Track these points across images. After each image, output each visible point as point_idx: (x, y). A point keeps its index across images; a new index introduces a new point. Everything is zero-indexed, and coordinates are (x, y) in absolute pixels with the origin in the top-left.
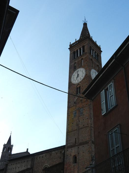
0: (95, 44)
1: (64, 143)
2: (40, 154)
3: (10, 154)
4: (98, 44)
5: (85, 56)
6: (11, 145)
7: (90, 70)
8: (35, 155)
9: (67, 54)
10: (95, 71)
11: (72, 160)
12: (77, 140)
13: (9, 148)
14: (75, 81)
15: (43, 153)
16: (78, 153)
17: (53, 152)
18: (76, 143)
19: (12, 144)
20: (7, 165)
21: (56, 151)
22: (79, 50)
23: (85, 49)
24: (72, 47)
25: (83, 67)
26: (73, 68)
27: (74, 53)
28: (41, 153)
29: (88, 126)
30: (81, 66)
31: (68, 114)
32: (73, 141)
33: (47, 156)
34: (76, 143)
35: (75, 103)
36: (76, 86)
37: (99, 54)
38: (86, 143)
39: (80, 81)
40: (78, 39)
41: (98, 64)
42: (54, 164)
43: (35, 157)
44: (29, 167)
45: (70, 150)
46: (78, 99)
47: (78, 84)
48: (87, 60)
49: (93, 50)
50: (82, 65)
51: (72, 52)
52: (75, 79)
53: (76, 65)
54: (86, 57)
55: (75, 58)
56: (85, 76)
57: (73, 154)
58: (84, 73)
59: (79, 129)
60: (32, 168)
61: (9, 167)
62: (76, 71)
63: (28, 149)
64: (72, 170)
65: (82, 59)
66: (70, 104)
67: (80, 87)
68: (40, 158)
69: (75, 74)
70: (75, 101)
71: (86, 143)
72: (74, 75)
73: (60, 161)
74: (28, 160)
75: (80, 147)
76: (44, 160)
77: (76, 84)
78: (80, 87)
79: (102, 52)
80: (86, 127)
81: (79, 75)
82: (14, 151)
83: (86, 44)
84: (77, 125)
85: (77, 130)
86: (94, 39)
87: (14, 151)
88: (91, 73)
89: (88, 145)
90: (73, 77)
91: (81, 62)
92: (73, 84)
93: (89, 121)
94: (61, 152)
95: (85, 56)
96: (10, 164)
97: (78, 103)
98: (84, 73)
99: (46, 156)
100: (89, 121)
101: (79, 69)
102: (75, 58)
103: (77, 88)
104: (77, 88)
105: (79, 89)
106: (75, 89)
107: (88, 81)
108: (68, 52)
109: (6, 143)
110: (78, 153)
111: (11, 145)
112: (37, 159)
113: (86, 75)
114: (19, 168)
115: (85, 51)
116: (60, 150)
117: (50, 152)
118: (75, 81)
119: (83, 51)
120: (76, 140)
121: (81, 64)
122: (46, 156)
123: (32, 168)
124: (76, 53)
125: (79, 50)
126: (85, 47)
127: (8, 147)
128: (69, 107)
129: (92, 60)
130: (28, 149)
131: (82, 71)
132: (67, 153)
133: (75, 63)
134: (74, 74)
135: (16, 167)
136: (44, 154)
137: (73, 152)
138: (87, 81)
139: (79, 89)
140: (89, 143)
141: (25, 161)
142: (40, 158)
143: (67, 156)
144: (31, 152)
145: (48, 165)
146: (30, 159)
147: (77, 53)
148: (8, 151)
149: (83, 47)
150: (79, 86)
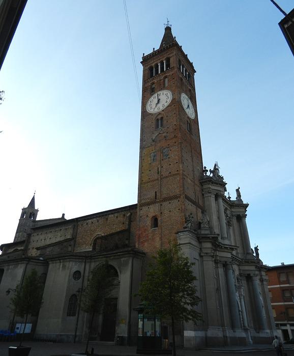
1: (134, 201)
2: (88, 219)
3: (35, 221)
5: (171, 73)
6: (36, 209)
7: (180, 94)
8: (80, 221)
9: (139, 70)
10: (186, 97)
11: (149, 222)
12: (157, 194)
13: (31, 213)
14: (154, 107)
15: (94, 218)
16: (161, 213)
17: (110, 216)
18: (156, 198)
19: (36, 208)
20: (29, 235)
21: (116, 215)
22: (159, 64)
24: (146, 60)
25: (167, 89)
26: (149, 90)
27: (151, 69)
28: (89, 218)
29: (178, 174)
30: (163, 87)
31: (141, 157)
32: (151, 195)
33: (100, 221)
34: (156, 198)
35: (153, 141)
36: (155, 116)
38: (176, 197)
39: (161, 108)
40: (157, 48)
42: (113, 231)
43: (79, 223)
44: (69, 237)
45: (145, 209)
46: (160, 135)
47: (160, 114)
48: (175, 79)
49: (183, 67)
50: (166, 85)
52: (154, 106)
53: (154, 86)
54: (173, 74)
55: (152, 76)
57: (151, 215)
58: (170, 97)
59: (161, 179)
60: (74, 238)
61: (32, 238)
62: (156, 95)
63: (63, 215)
64: (150, 237)
65: (166, 77)
66: (144, 143)
67: (162, 118)
68: (87, 224)
69: (153, 100)
70: (154, 138)
71: (176, 197)
73: (123, 228)
74: (67, 227)
75: (164, 204)
76: (95, 227)
77: (155, 114)
78: (162, 118)
80: (176, 174)
81: (161, 101)
82: (39, 218)
84: (158, 173)
85: (158, 179)
87: (39, 218)
88: (182, 98)
89: (179, 201)
90: (149, 103)
91: (164, 81)
92: (150, 114)
93: (181, 167)
94: (124, 215)
95: (171, 73)
96: (35, 234)
97: (160, 141)
98: (170, 97)
99: (98, 221)
100: (181, 167)
101: (161, 92)
102: (152, 76)
103: (158, 119)
106: (154, 121)
107: (177, 109)
108: (141, 68)
109: (26, 206)
110: (161, 213)
111: (36, 209)
112: (82, 225)
113: (173, 100)
114: (50, 239)
115: (171, 64)
116: (123, 213)
117: (106, 215)
119: (168, 66)
120: (156, 195)
121: (164, 84)
122: (98, 221)
123: (74, 238)
125: (159, 64)
126: (171, 60)
127: (30, 212)
128: (142, 148)
129: (182, 80)
130: (63, 215)
131: (167, 95)
132: (140, 214)
133: (153, 83)
134: (152, 98)
135: (46, 238)
136: (95, 219)
137: (153, 210)
138: (176, 108)
139: (160, 121)
140: (180, 197)
141: (61, 230)
142: (87, 224)
143: (141, 217)
144: (67, 218)
145: (101, 233)
146: (70, 226)
148: (30, 217)
149: (168, 60)
150: (159, 117)
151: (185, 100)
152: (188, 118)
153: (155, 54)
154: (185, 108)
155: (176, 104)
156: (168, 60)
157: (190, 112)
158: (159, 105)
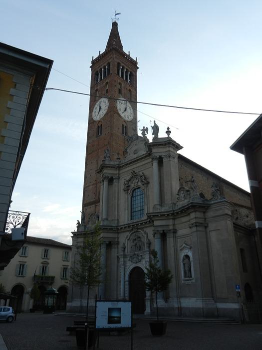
0: (127, 58)
4: (133, 56)
14: (97, 117)
23: (111, 66)
24: (94, 62)
26: (94, 98)
37: (133, 73)
39: (102, 116)
40: (103, 50)
47: (99, 121)
51: (94, 73)
67: (101, 125)
69: (97, 107)
78: (101, 125)
79: (138, 68)
83: (115, 59)
86: (126, 50)
90: (94, 111)
104: (99, 126)
134: (96, 106)
149: (109, 64)
150: (100, 125)
151: (121, 105)
153: (101, 57)
154: (120, 112)
155: (112, 111)
156: (109, 64)
157: (127, 116)
158: (101, 112)
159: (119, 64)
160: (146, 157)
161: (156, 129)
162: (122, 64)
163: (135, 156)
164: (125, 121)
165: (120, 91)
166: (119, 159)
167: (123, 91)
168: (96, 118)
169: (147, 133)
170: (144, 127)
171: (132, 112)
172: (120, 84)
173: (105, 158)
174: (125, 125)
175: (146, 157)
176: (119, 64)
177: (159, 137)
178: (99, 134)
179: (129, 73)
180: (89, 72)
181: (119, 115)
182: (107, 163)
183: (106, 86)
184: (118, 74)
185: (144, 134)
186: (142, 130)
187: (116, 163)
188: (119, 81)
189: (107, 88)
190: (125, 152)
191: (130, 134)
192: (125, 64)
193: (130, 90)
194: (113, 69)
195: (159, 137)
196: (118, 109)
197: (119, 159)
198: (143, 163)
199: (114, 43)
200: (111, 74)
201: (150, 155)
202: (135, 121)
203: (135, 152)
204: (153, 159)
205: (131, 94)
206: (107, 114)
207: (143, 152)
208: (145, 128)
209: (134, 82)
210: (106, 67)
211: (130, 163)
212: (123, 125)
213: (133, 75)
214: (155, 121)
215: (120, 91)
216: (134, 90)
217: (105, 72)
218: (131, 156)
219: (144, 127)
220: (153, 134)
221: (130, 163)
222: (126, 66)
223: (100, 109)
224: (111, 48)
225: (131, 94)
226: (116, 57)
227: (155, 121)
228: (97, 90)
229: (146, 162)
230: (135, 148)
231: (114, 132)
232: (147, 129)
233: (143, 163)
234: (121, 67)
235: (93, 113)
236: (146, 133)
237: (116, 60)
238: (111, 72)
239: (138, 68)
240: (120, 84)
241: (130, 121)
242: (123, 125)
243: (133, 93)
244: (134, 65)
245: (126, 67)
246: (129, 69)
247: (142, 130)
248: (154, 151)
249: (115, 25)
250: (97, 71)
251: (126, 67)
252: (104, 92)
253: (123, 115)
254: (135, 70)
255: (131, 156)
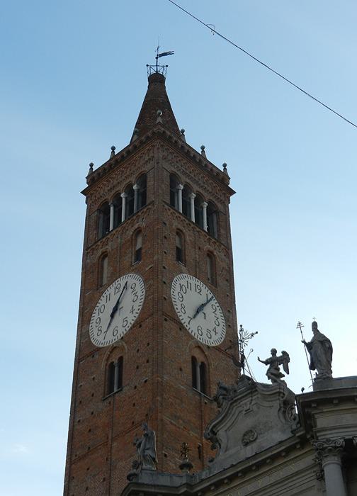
0: (198, 161)
4: (216, 159)
10: (194, 281)
14: (104, 337)
23: (150, 183)
24: (96, 179)
37: (219, 205)
39: (122, 331)
40: (123, 141)
41: (212, 249)
47: (113, 348)
51: (96, 207)
56: (142, 309)
58: (139, 294)
67: (121, 359)
69: (106, 303)
72: (100, 310)
77: (109, 346)
78: (121, 359)
79: (232, 192)
83: (159, 162)
86: (193, 140)
88: (175, 291)
90: (95, 316)
92: (99, 349)
98: (139, 294)
104: (112, 366)
105: (116, 369)
118: (103, 335)
124: (112, 208)
139: (116, 369)
147: (115, 207)
149: (143, 179)
152: (199, 347)
153: (118, 161)
154: (184, 319)
157: (206, 329)
159: (174, 180)
160: (288, 451)
161: (320, 350)
162: (184, 179)
163: (249, 451)
164: (199, 347)
165: (180, 255)
166: (189, 466)
167: (191, 254)
168: (100, 338)
169: (287, 370)
170: (274, 352)
171: (221, 321)
172: (179, 233)
173: (136, 465)
174: (200, 358)
175: (288, 451)
176: (174, 180)
177: (335, 375)
178: (111, 389)
179: (206, 204)
180: (79, 208)
181: (181, 327)
182: (145, 479)
183: (133, 240)
184: (173, 203)
185: (274, 374)
186: (266, 363)
187: (178, 481)
188: (176, 224)
189: (139, 246)
190: (214, 441)
191: (217, 377)
192: (191, 178)
193: (210, 255)
194: (157, 191)
195: (335, 375)
196: (178, 306)
197: (189, 466)
198: (282, 474)
199: (159, 120)
200: (152, 203)
201: (303, 442)
202: (231, 348)
203: (247, 441)
204: (322, 452)
205: (213, 265)
206: (138, 324)
207: (276, 434)
208: (279, 354)
209: (222, 231)
210: (135, 187)
211: (231, 478)
212: (194, 359)
213: (217, 212)
214: (315, 325)
215: (180, 255)
216: (222, 255)
217: (130, 204)
218: (233, 453)
219: (274, 352)
220: (312, 367)
221: (231, 478)
222: (197, 183)
223: (115, 310)
224: (149, 134)
225: (213, 265)
226: (165, 158)
227: (315, 325)
228: (105, 255)
229: (293, 468)
230: (245, 424)
231: (166, 377)
232: (285, 358)
233: (282, 474)
234: (182, 187)
235: (93, 324)
236: (282, 371)
237: (166, 165)
238: (150, 197)
239: (232, 192)
240: (179, 233)
241: (216, 348)
242: (194, 359)
243: (221, 264)
244: (219, 183)
245: (196, 188)
246: (205, 194)
247: (266, 363)
248: (322, 421)
249: (157, 81)
250: (107, 203)
251: (196, 188)
252: (128, 258)
253: (192, 327)
254: (222, 198)
255: (232, 451)
